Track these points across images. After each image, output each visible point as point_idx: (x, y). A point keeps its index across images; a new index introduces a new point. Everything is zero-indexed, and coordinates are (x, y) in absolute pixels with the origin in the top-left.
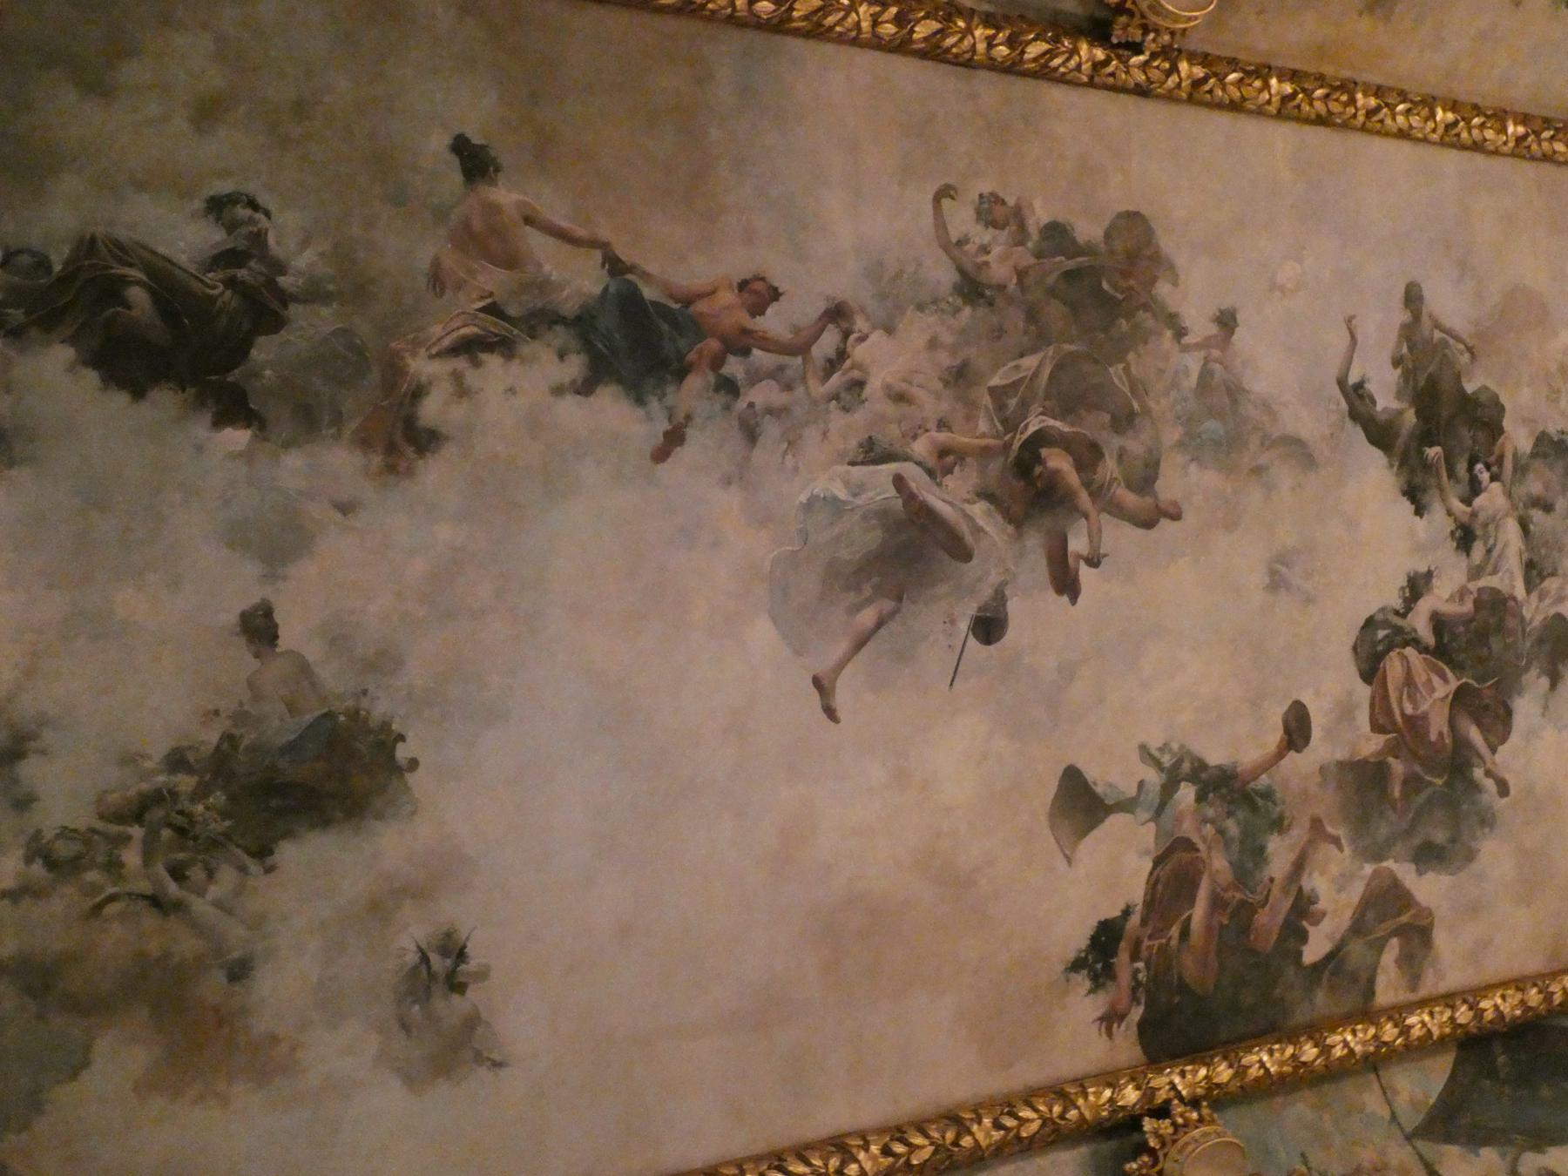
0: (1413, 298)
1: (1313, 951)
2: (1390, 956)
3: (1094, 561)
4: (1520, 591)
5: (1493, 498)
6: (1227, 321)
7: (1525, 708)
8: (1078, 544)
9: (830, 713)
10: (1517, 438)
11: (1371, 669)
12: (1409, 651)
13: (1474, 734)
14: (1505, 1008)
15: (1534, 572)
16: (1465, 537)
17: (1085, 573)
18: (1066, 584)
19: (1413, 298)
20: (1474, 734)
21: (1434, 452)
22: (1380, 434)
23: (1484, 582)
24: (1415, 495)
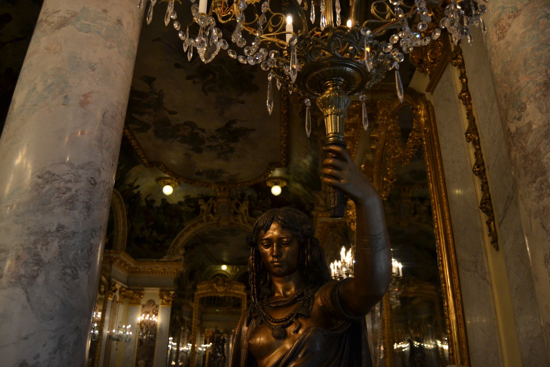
0: (253, 130)
1: (134, 115)
2: (137, 126)
3: (194, 82)
4: (206, 145)
5: (221, 141)
6: (242, 102)
7: (186, 146)
8: (196, 80)
9: (154, 41)
10: (232, 145)
11: (185, 124)
12: (191, 129)
13: (179, 139)
14: (133, 144)
15: (210, 147)
16: (213, 137)
17: (192, 81)
18: (188, 78)
19: (253, 130)
20: (179, 139)
21: (227, 133)
22: (228, 125)
23: (207, 141)
24: (218, 130)
